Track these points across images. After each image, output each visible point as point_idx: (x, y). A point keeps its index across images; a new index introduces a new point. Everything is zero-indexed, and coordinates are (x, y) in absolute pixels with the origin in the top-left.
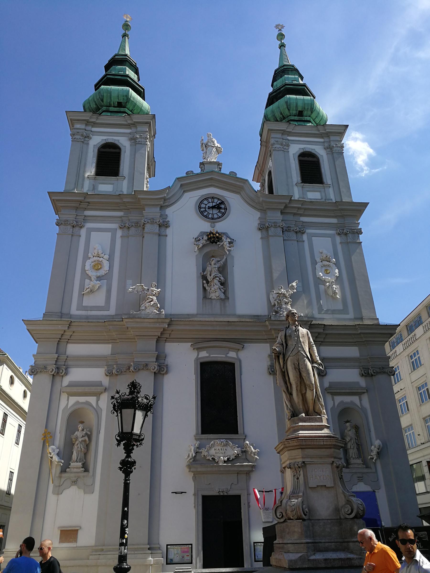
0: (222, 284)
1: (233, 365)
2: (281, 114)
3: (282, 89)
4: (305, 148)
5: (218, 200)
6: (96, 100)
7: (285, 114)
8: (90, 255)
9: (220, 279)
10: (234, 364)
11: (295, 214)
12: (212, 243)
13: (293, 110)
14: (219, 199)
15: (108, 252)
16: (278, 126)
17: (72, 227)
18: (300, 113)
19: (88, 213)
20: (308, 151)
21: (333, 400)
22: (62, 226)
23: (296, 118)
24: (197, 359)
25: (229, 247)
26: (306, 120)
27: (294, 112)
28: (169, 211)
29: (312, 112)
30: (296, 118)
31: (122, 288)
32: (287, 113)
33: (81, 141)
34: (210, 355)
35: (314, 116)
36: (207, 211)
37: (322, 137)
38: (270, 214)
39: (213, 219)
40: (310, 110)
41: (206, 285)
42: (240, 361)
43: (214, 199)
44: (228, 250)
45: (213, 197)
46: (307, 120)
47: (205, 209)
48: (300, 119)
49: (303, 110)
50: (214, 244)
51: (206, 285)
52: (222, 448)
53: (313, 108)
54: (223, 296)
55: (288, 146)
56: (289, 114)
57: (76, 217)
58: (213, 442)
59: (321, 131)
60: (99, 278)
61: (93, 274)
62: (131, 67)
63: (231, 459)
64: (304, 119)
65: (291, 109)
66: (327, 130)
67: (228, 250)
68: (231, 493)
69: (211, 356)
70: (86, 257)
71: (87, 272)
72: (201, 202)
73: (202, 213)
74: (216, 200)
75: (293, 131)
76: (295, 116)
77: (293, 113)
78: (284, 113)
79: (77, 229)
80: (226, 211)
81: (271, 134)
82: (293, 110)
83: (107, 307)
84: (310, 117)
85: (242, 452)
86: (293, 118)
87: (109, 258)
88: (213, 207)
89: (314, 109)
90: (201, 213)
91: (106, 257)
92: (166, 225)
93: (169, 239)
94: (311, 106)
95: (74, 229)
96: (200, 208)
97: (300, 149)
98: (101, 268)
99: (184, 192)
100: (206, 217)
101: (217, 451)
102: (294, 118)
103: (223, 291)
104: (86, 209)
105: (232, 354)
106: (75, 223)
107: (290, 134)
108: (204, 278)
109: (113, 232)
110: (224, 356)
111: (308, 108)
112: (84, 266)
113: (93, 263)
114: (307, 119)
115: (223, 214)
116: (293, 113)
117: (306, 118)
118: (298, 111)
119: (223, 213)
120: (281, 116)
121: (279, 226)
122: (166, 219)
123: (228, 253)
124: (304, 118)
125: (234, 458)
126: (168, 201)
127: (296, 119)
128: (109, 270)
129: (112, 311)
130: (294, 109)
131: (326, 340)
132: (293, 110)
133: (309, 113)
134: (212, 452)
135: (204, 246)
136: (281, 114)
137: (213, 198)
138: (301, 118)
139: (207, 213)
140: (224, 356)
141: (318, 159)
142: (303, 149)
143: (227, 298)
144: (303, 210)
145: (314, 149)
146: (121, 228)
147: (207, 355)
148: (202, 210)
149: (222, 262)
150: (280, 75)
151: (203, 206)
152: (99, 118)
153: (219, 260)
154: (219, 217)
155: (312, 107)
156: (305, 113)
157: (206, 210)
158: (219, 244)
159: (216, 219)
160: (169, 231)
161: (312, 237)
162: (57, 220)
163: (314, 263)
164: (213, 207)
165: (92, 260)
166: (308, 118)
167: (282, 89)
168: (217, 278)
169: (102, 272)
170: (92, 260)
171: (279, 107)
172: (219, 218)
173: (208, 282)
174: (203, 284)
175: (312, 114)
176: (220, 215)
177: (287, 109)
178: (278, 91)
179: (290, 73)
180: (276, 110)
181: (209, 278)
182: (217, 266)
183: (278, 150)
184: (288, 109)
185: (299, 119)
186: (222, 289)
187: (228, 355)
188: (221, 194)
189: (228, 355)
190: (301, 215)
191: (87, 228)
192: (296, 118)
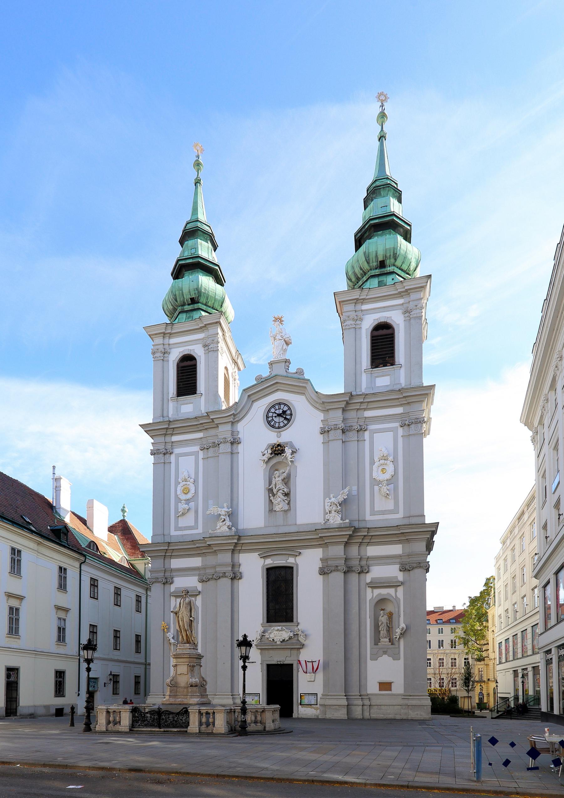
0: (287, 495)
1: (292, 568)
3: (366, 227)
4: (379, 318)
5: (285, 405)
7: (365, 269)
8: (179, 480)
9: (284, 491)
10: (292, 568)
11: (358, 409)
12: (277, 454)
13: (373, 262)
14: (285, 404)
15: (193, 476)
16: (350, 295)
17: (163, 455)
18: (382, 264)
19: (175, 438)
20: (382, 322)
21: (372, 592)
22: (156, 455)
23: (377, 272)
24: (263, 566)
25: (291, 458)
26: (388, 271)
27: (375, 264)
28: (240, 427)
29: (396, 260)
30: (377, 272)
31: (206, 508)
32: (366, 267)
33: (161, 360)
34: (273, 562)
35: (398, 263)
37: (402, 297)
38: (332, 414)
39: (279, 428)
40: (393, 257)
41: (272, 498)
42: (297, 565)
44: (291, 461)
45: (279, 403)
46: (390, 271)
48: (382, 273)
49: (385, 259)
50: (279, 455)
51: (272, 498)
52: (279, 633)
53: (396, 254)
54: (286, 507)
55: (361, 320)
56: (369, 268)
57: (165, 444)
58: (272, 629)
59: (399, 290)
60: (188, 501)
61: (183, 497)
62: (205, 235)
63: (286, 640)
64: (387, 271)
65: (371, 262)
66: (406, 288)
67: (291, 461)
68: (286, 662)
69: (274, 562)
70: (177, 483)
71: (179, 496)
72: (268, 411)
74: (282, 406)
75: (368, 297)
76: (376, 269)
77: (373, 266)
78: (363, 268)
79: (167, 456)
81: (344, 306)
82: (373, 262)
83: (196, 527)
84: (394, 265)
85: (294, 635)
86: (373, 272)
87: (194, 482)
88: (279, 415)
89: (398, 254)
90: (268, 423)
91: (192, 480)
92: (237, 442)
93: (240, 456)
94: (394, 251)
95: (165, 456)
96: (267, 417)
97: (374, 320)
98: (189, 492)
99: (252, 401)
100: (273, 427)
101: (276, 635)
102: (375, 273)
103: (287, 502)
104: (172, 435)
105: (291, 561)
106: (165, 451)
107: (365, 301)
108: (270, 491)
109: (196, 454)
110: (285, 562)
111: (390, 255)
112: (176, 491)
113: (183, 488)
114: (390, 270)
115: (289, 420)
116: (373, 266)
117: (388, 269)
118: (379, 262)
120: (362, 272)
121: (339, 428)
122: (238, 435)
123: (290, 463)
124: (386, 269)
125: (288, 639)
126: (238, 415)
127: (377, 274)
128: (195, 493)
129: (200, 530)
131: (372, 541)
133: (392, 260)
134: (272, 636)
135: (270, 459)
138: (383, 270)
139: (274, 422)
140: (285, 562)
141: (393, 329)
142: (377, 319)
143: (289, 510)
144: (367, 404)
145: (391, 317)
146: (202, 450)
147: (272, 562)
148: (270, 419)
149: (285, 474)
150: (371, 197)
151: (270, 414)
152: (173, 327)
153: (284, 471)
154: (285, 425)
155: (395, 253)
156: (388, 262)
158: (283, 455)
160: (240, 447)
161: (374, 433)
162: (151, 450)
163: (372, 463)
164: (279, 415)
165: (181, 484)
166: (391, 269)
167: (366, 227)
168: (281, 491)
169: (189, 496)
170: (181, 484)
172: (285, 426)
173: (274, 495)
174: (270, 497)
175: (396, 261)
176: (286, 422)
177: (366, 263)
178: (363, 230)
179: (382, 193)
180: (355, 265)
181: (275, 491)
182: (280, 479)
183: (349, 328)
184: (367, 262)
185: (381, 272)
186: (285, 500)
187: (288, 561)
188: (286, 399)
189: (288, 561)
190: (365, 409)
191: (175, 454)
192: (377, 272)
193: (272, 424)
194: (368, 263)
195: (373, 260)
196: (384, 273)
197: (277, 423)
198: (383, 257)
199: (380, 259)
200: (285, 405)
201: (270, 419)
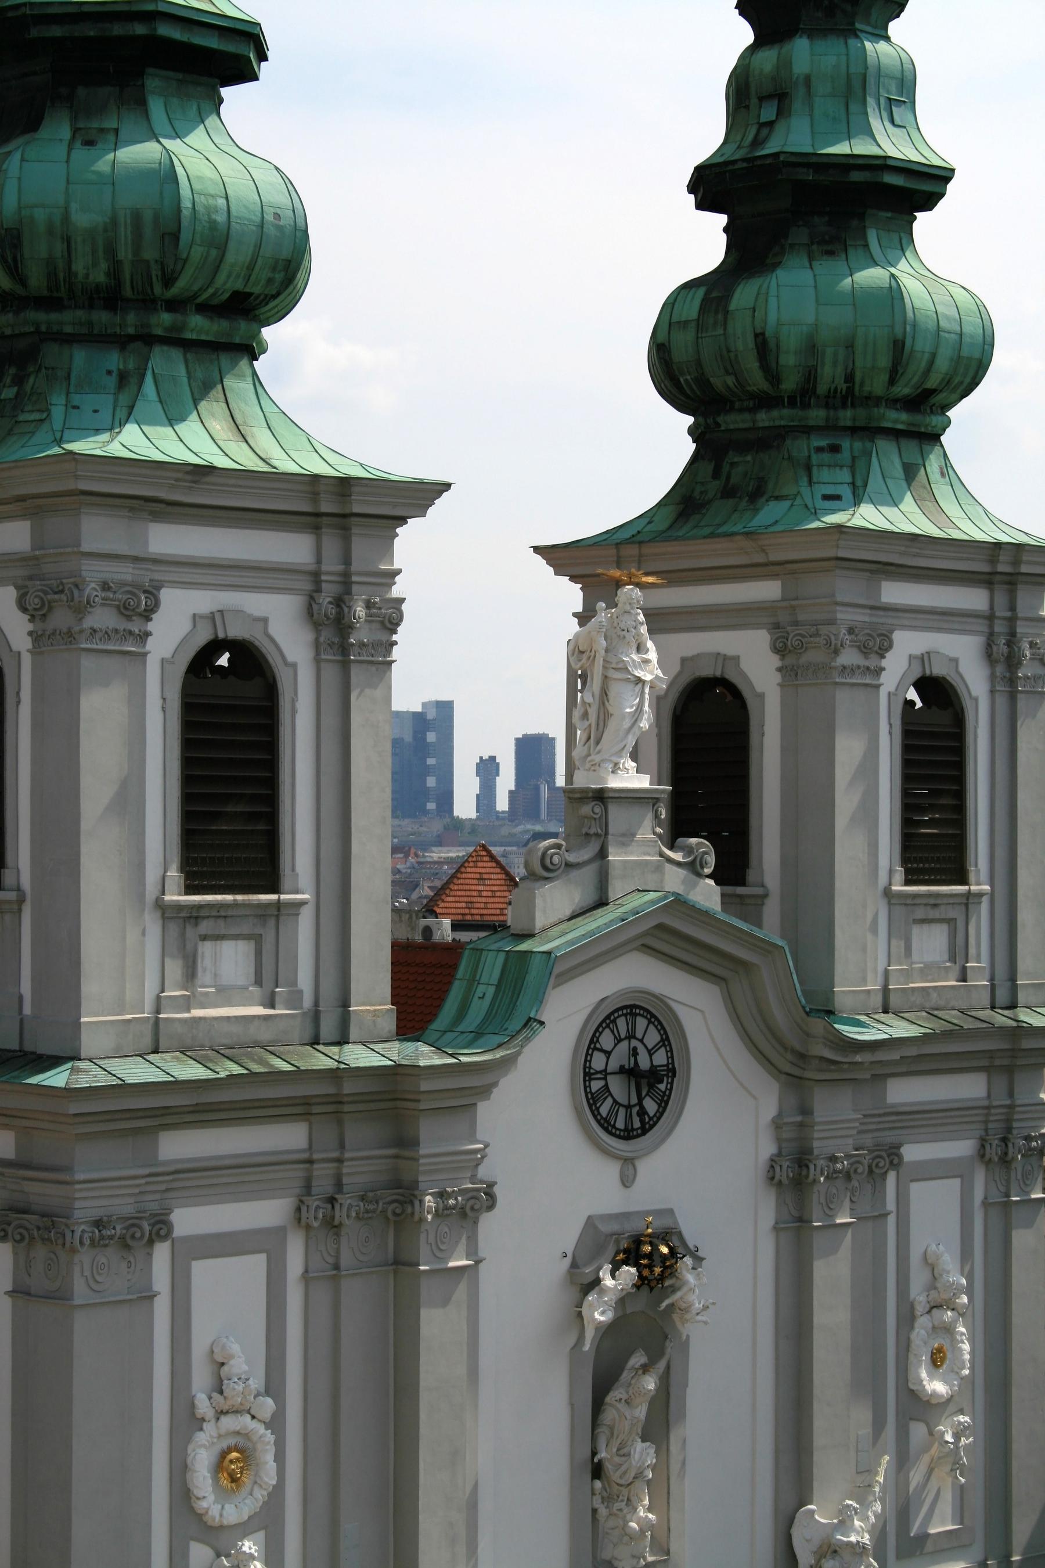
2: (850, 378)
6: (125, 253)
36: (611, 1094)
43: (636, 1015)
47: (605, 1079)
73: (595, 1103)
78: (862, 384)
80: (672, 1083)
119: (663, 1097)
130: (915, 379)
132: (906, 385)
136: (850, 378)
137: (631, 1014)
139: (609, 1101)
157: (606, 1085)
159: (587, 1054)
171: (850, 346)
193: (620, 1124)
194: (892, 381)
195: (911, 379)
196: (916, 429)
197: (622, 1112)
198: (940, 383)
199: (932, 383)
200: (652, 1018)
201: (596, 1085)
